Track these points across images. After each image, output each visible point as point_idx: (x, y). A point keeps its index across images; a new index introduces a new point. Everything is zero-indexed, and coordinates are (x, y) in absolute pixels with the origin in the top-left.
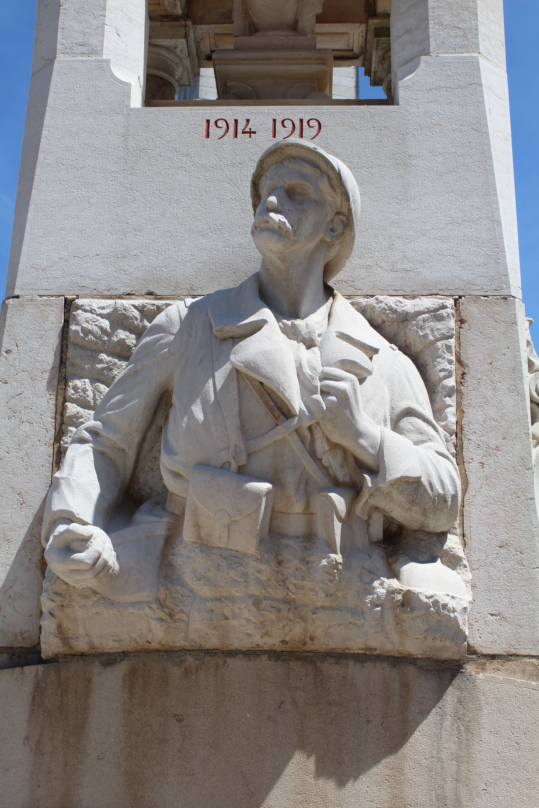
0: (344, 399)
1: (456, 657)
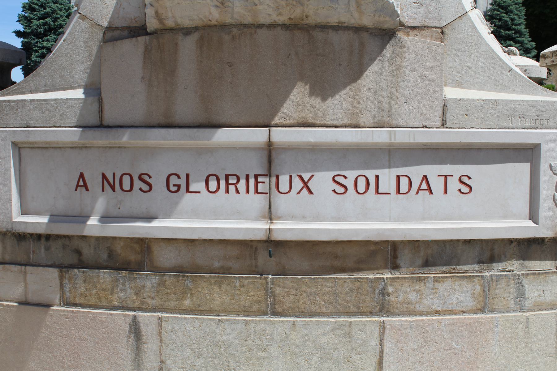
1: (392, 27)
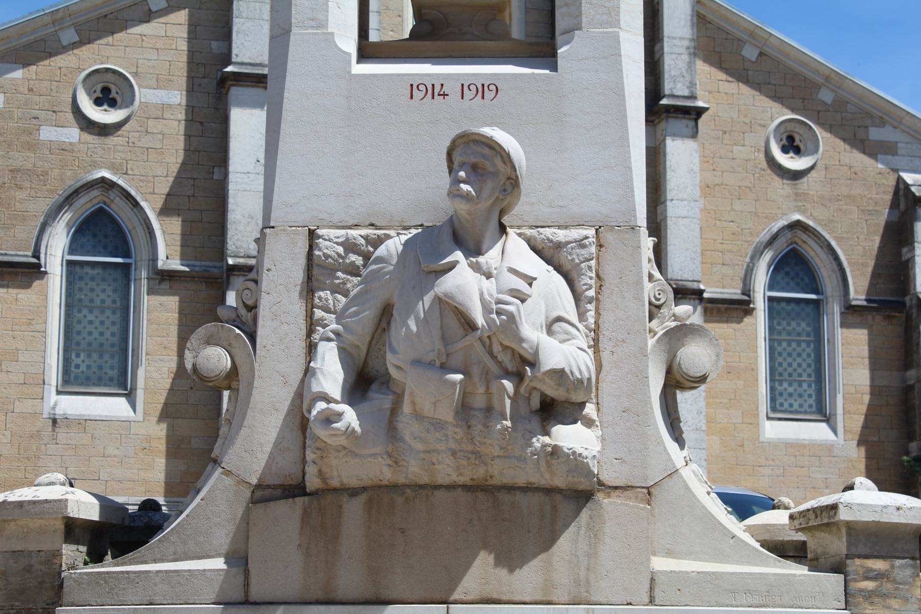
0: (512, 318)
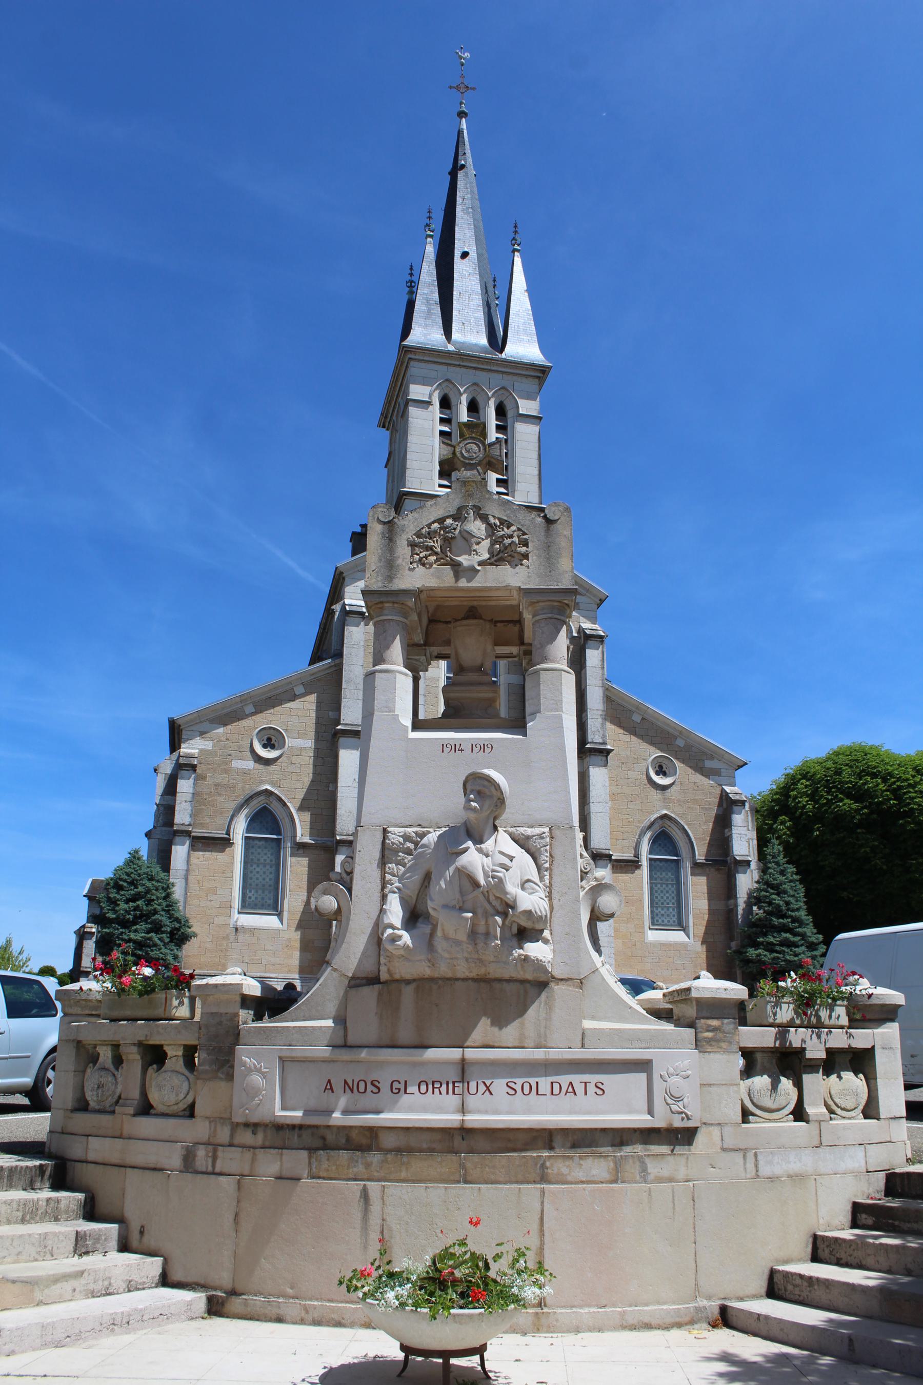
0: (501, 881)
